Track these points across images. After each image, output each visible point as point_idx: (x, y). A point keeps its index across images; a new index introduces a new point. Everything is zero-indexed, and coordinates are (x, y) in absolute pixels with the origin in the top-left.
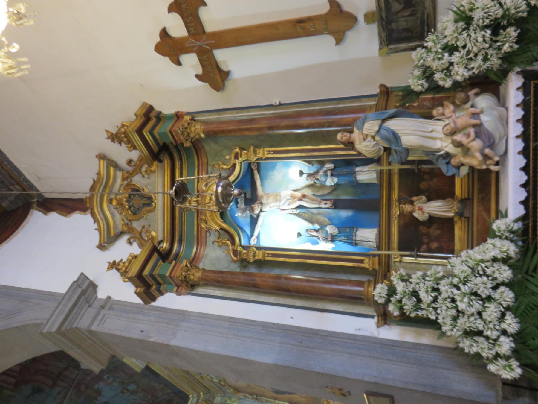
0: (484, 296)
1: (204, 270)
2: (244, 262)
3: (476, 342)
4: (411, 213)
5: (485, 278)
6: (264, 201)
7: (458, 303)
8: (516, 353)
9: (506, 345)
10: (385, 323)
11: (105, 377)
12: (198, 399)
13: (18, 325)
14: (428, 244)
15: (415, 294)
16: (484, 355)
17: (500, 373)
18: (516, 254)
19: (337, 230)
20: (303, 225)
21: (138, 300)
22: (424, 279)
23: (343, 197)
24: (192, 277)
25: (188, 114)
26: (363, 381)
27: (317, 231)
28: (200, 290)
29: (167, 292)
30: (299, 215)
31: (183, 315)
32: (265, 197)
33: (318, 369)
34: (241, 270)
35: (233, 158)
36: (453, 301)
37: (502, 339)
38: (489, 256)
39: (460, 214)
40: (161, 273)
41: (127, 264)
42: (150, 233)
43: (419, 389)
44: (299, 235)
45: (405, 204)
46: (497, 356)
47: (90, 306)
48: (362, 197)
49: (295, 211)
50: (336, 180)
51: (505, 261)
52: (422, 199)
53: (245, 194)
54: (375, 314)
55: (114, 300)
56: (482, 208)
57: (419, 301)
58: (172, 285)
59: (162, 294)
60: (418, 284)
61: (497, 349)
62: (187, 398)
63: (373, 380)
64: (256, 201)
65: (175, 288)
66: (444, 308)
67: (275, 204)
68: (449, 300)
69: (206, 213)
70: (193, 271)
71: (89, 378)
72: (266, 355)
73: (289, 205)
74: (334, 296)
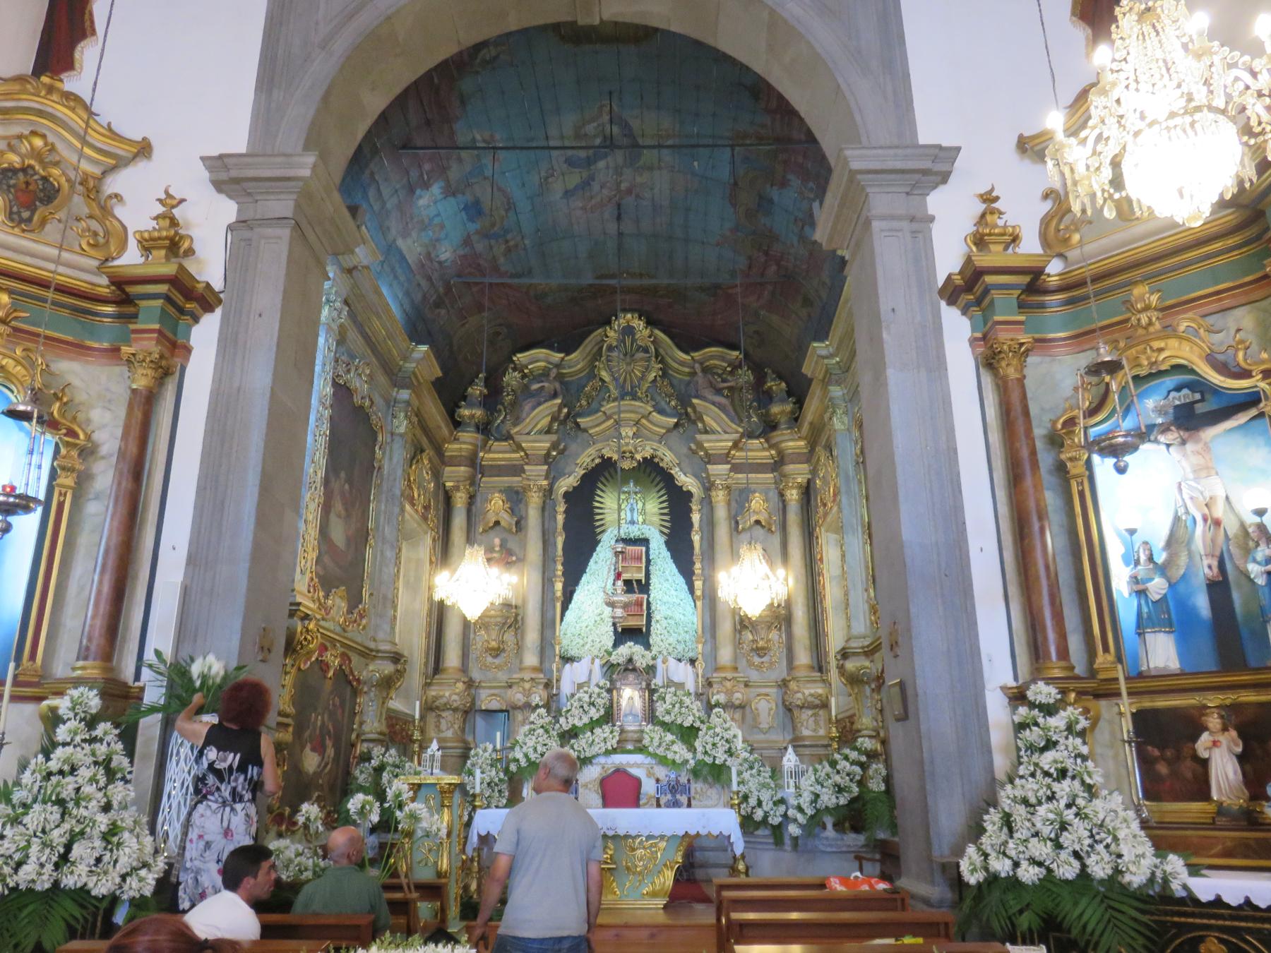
0: (1061, 840)
1: (1021, 381)
2: (1055, 441)
3: (1001, 829)
4: (1206, 729)
5: (1088, 841)
6: (1189, 447)
7: (1045, 806)
8: (993, 879)
9: (1002, 866)
10: (1010, 699)
11: (811, 184)
12: (827, 357)
13: (844, 87)
14: (1163, 758)
15: (1050, 745)
16: (984, 839)
17: (966, 859)
18: (1129, 883)
19: (1158, 597)
20: (1158, 532)
21: (941, 281)
22: (1076, 757)
23: (1236, 596)
24: (1004, 364)
26: (914, 676)
27: (1150, 558)
28: (987, 379)
29: (970, 319)
30: (1177, 519)
31: (936, 364)
32: (1199, 447)
33: (913, 610)
34: (1045, 436)
35: (1263, 367)
36: (1051, 798)
37: (1008, 863)
38: (1124, 849)
39: (1221, 810)
40: (997, 303)
41: (997, 231)
42: (1077, 230)
43: (925, 755)
44: (1132, 532)
45: (1222, 717)
46: (986, 855)
47: (907, 194)
48: (1245, 632)
49: (1181, 511)
50: (1261, 581)
51: (1117, 871)
52: (1237, 745)
53: (1202, 400)
54: (1021, 682)
55: (930, 231)
56: (1229, 844)
57: (1043, 750)
58: (985, 324)
59: (964, 312)
60: (1067, 749)
61: (993, 855)
62: (822, 335)
63: (920, 692)
64: (1187, 429)
65: (979, 335)
66: (1035, 787)
67: (1188, 470)
68: (1049, 793)
69: (1130, 347)
70: (1015, 362)
71: (800, 160)
72: (914, 525)
73: (1192, 498)
74: (1031, 613)
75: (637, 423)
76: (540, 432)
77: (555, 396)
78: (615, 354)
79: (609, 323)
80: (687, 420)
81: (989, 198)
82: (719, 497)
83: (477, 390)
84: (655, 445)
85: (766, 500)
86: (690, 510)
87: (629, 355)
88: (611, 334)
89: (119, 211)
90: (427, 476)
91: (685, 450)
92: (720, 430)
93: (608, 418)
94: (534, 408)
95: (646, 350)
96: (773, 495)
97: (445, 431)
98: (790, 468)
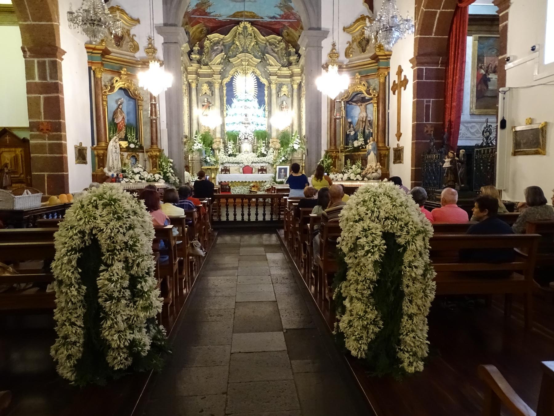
25: (389, 73)
75: (248, 60)
76: (217, 64)
77: (222, 52)
78: (241, 36)
79: (239, 24)
80: (263, 59)
81: (334, 45)
82: (273, 87)
83: (196, 48)
84: (254, 68)
85: (287, 88)
86: (264, 90)
87: (246, 37)
88: (239, 28)
89: (135, 38)
90: (185, 80)
91: (263, 70)
92: (274, 66)
93: (239, 58)
94: (216, 56)
95: (251, 35)
96: (290, 85)
97: (189, 64)
98: (295, 78)
